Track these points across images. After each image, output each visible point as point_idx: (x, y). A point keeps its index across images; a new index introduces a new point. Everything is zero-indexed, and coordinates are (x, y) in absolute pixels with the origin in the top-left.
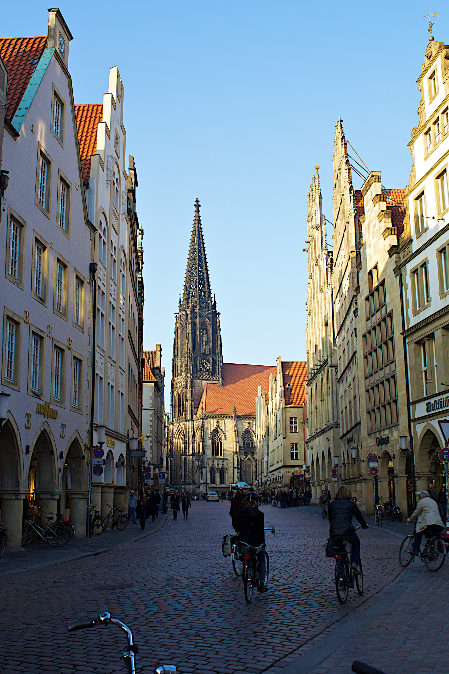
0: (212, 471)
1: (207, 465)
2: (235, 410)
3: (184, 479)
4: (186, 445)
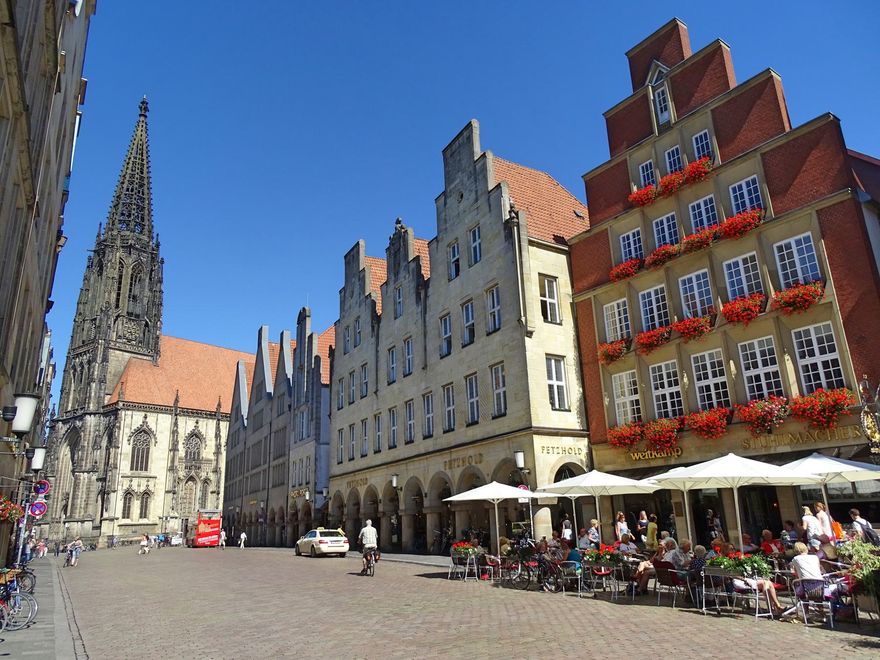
0: (128, 495)
1: (120, 487)
2: (177, 401)
3: (72, 512)
4: (83, 454)
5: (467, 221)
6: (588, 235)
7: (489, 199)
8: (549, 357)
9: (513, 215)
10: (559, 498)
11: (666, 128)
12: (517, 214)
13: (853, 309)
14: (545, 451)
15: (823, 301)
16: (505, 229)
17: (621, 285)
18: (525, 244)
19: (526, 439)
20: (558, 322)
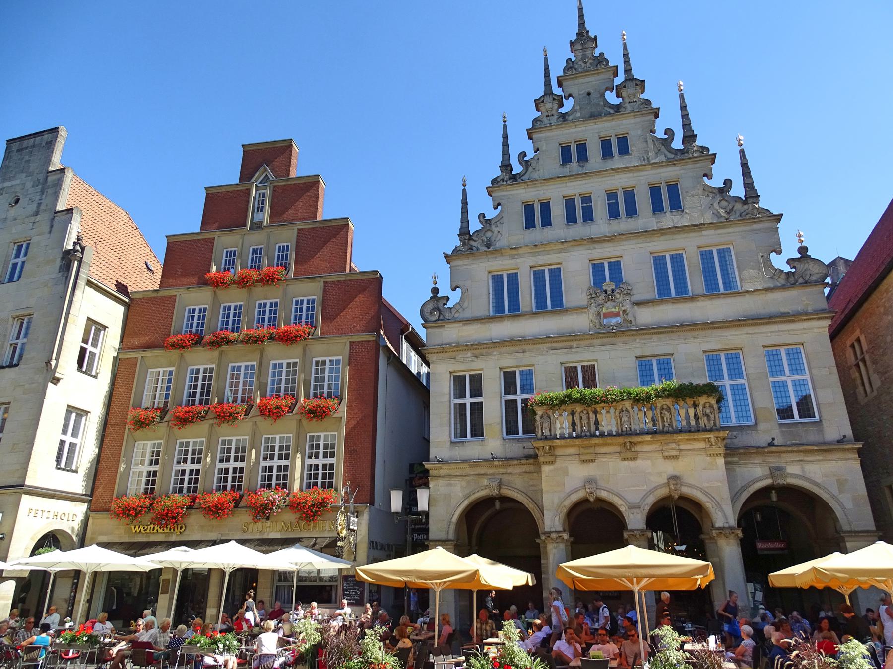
5: (14, 231)
6: (155, 295)
7: (53, 219)
8: (70, 409)
9: (78, 248)
10: (32, 571)
11: (257, 226)
12: (83, 249)
13: (355, 427)
14: (33, 514)
15: (336, 415)
16: (62, 259)
17: (175, 354)
18: (82, 283)
19: (12, 498)
20: (94, 373)
